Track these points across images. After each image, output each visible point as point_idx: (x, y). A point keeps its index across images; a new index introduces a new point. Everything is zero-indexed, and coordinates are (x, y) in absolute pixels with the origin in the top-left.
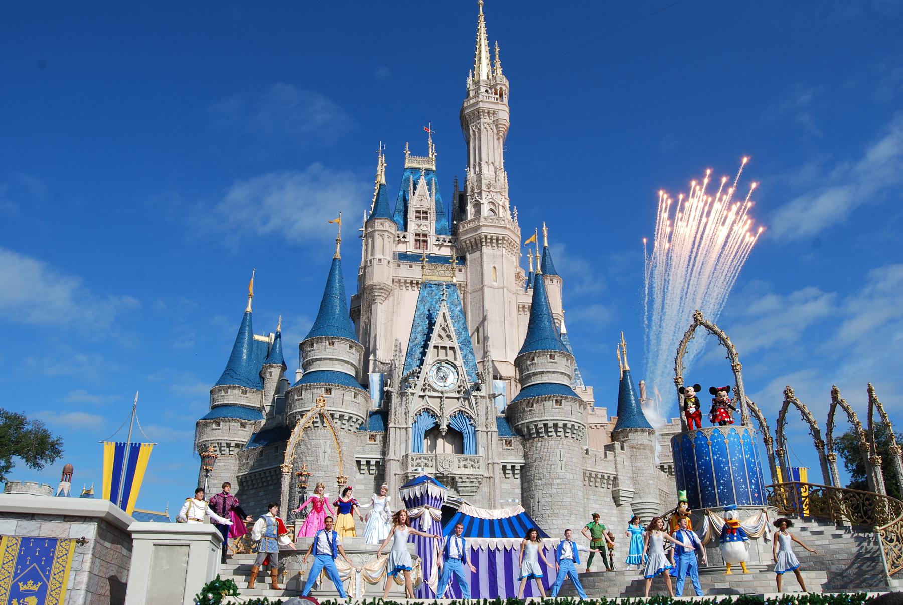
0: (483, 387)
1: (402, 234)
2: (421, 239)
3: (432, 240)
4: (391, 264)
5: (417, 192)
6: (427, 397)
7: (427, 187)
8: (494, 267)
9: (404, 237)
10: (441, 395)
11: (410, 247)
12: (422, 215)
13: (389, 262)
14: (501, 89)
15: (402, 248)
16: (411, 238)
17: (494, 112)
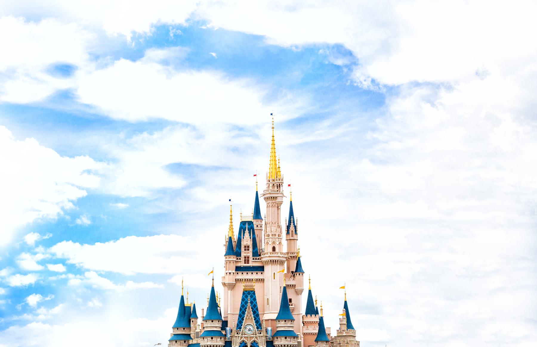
0: (262, 333)
1: (239, 258)
2: (247, 260)
3: (251, 260)
4: (234, 274)
5: (244, 237)
6: (243, 337)
7: (249, 234)
8: (274, 273)
9: (240, 259)
10: (248, 336)
11: (242, 264)
12: (247, 248)
13: (234, 273)
14: (279, 184)
15: (239, 265)
16: (243, 259)
17: (276, 197)
